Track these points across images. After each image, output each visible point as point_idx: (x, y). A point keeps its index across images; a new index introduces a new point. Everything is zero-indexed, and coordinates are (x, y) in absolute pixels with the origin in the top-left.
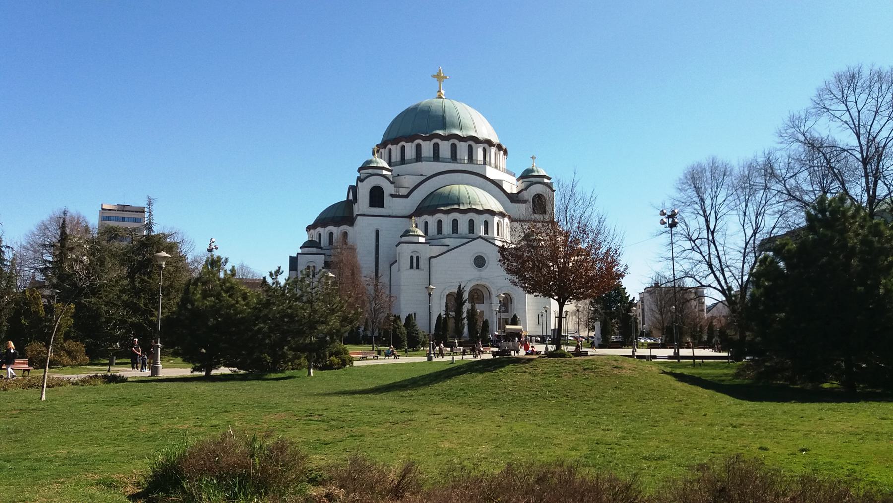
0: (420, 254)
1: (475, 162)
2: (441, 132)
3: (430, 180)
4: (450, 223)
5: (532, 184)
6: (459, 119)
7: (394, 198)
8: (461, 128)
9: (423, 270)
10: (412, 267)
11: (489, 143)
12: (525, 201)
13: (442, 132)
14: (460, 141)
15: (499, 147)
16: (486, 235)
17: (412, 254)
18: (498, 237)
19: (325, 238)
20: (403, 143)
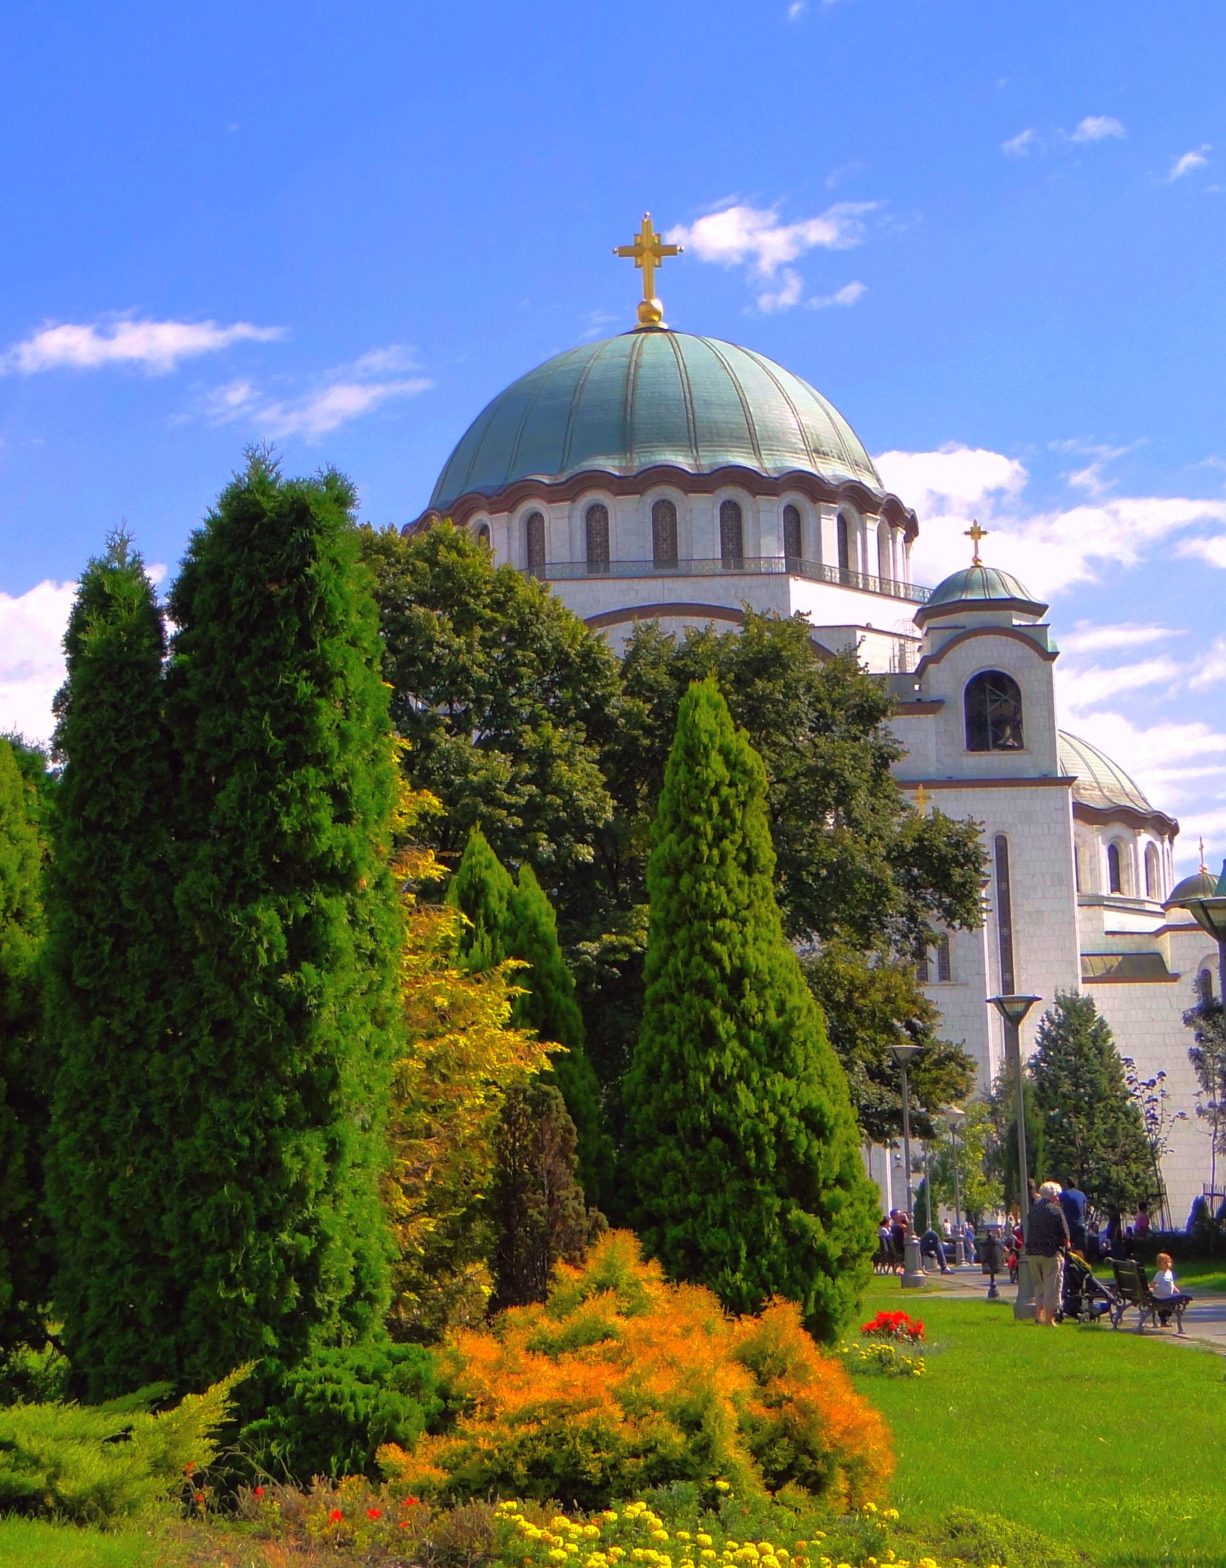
1: (750, 566)
5: (963, 635)
6: (688, 402)
13: (616, 463)
14: (687, 491)
20: (481, 517)
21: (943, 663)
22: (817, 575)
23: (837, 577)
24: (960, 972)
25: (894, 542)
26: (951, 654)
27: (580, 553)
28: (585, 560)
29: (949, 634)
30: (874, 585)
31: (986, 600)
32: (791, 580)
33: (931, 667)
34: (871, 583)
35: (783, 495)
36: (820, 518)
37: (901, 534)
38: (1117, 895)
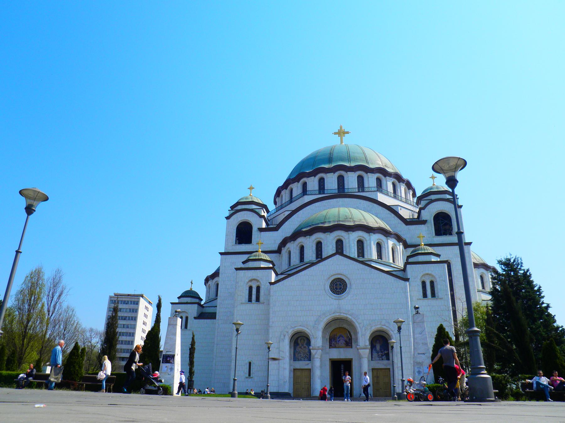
0: (260, 282)
2: (326, 166)
3: (304, 209)
4: (312, 246)
5: (432, 201)
6: (348, 152)
7: (262, 232)
8: (349, 160)
9: (264, 303)
10: (250, 300)
11: (382, 171)
12: (424, 222)
13: (327, 166)
15: (398, 178)
16: (361, 259)
17: (250, 284)
18: (379, 260)
19: (212, 289)
20: (291, 186)
21: (425, 210)
22: (387, 194)
23: (392, 195)
24: (440, 294)
25: (410, 194)
26: (428, 207)
27: (317, 187)
28: (318, 189)
29: (427, 201)
30: (404, 200)
31: (438, 191)
32: (378, 194)
33: (422, 211)
34: (403, 199)
35: (376, 174)
36: (387, 181)
37: (411, 193)
38: (484, 290)
